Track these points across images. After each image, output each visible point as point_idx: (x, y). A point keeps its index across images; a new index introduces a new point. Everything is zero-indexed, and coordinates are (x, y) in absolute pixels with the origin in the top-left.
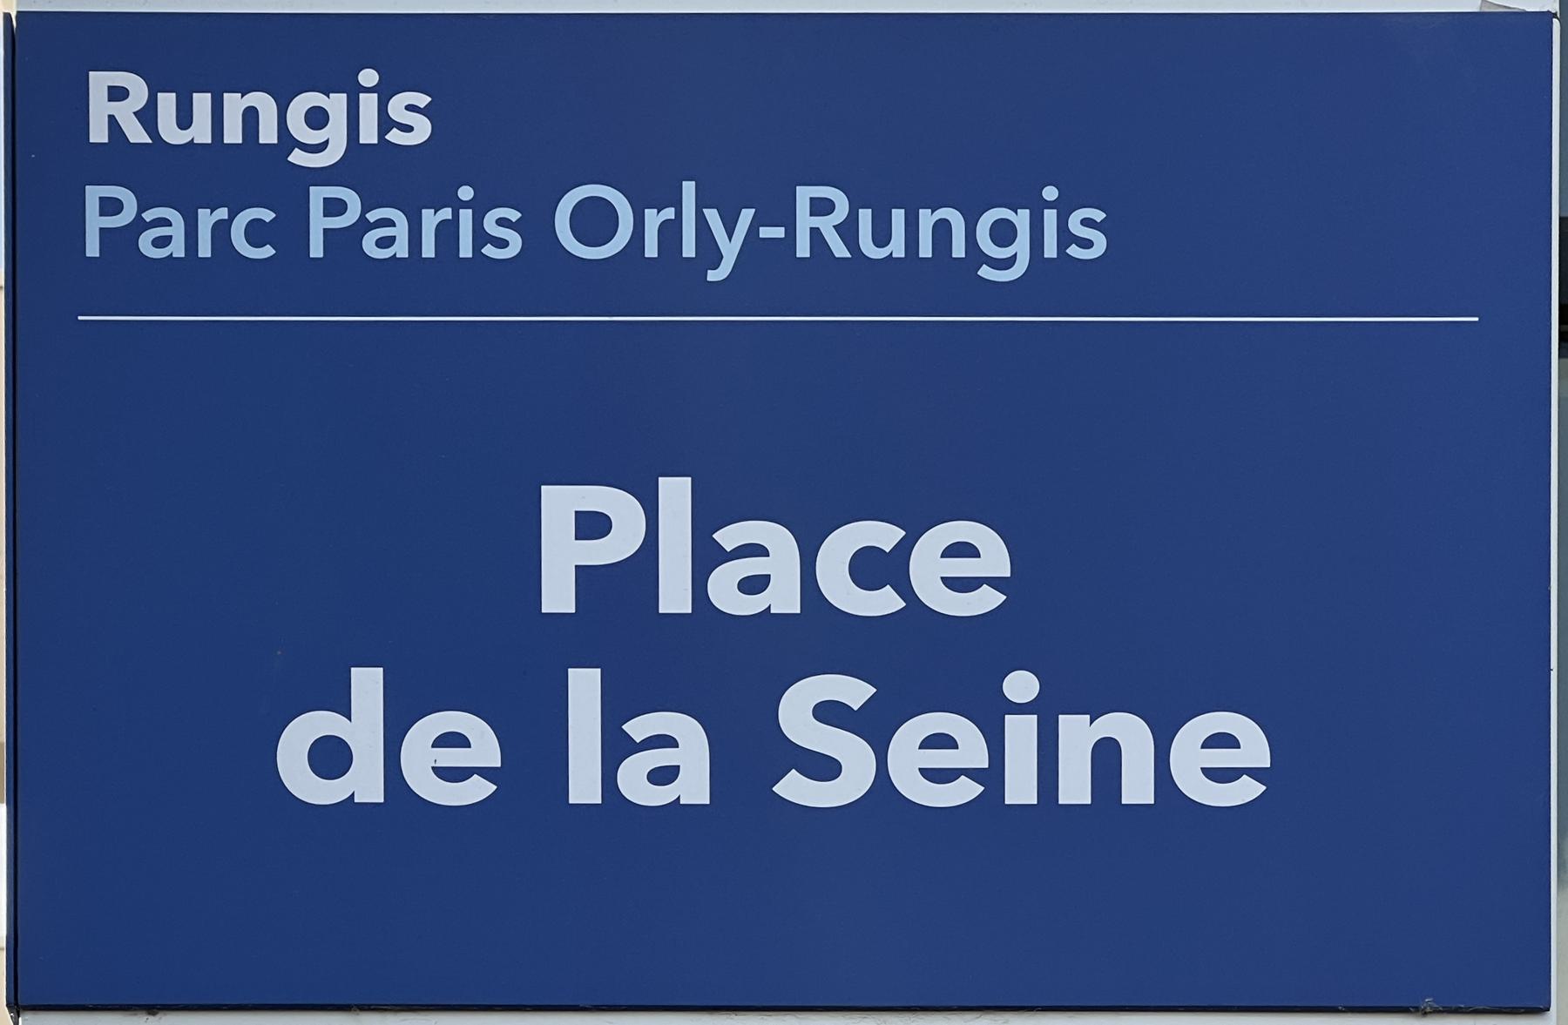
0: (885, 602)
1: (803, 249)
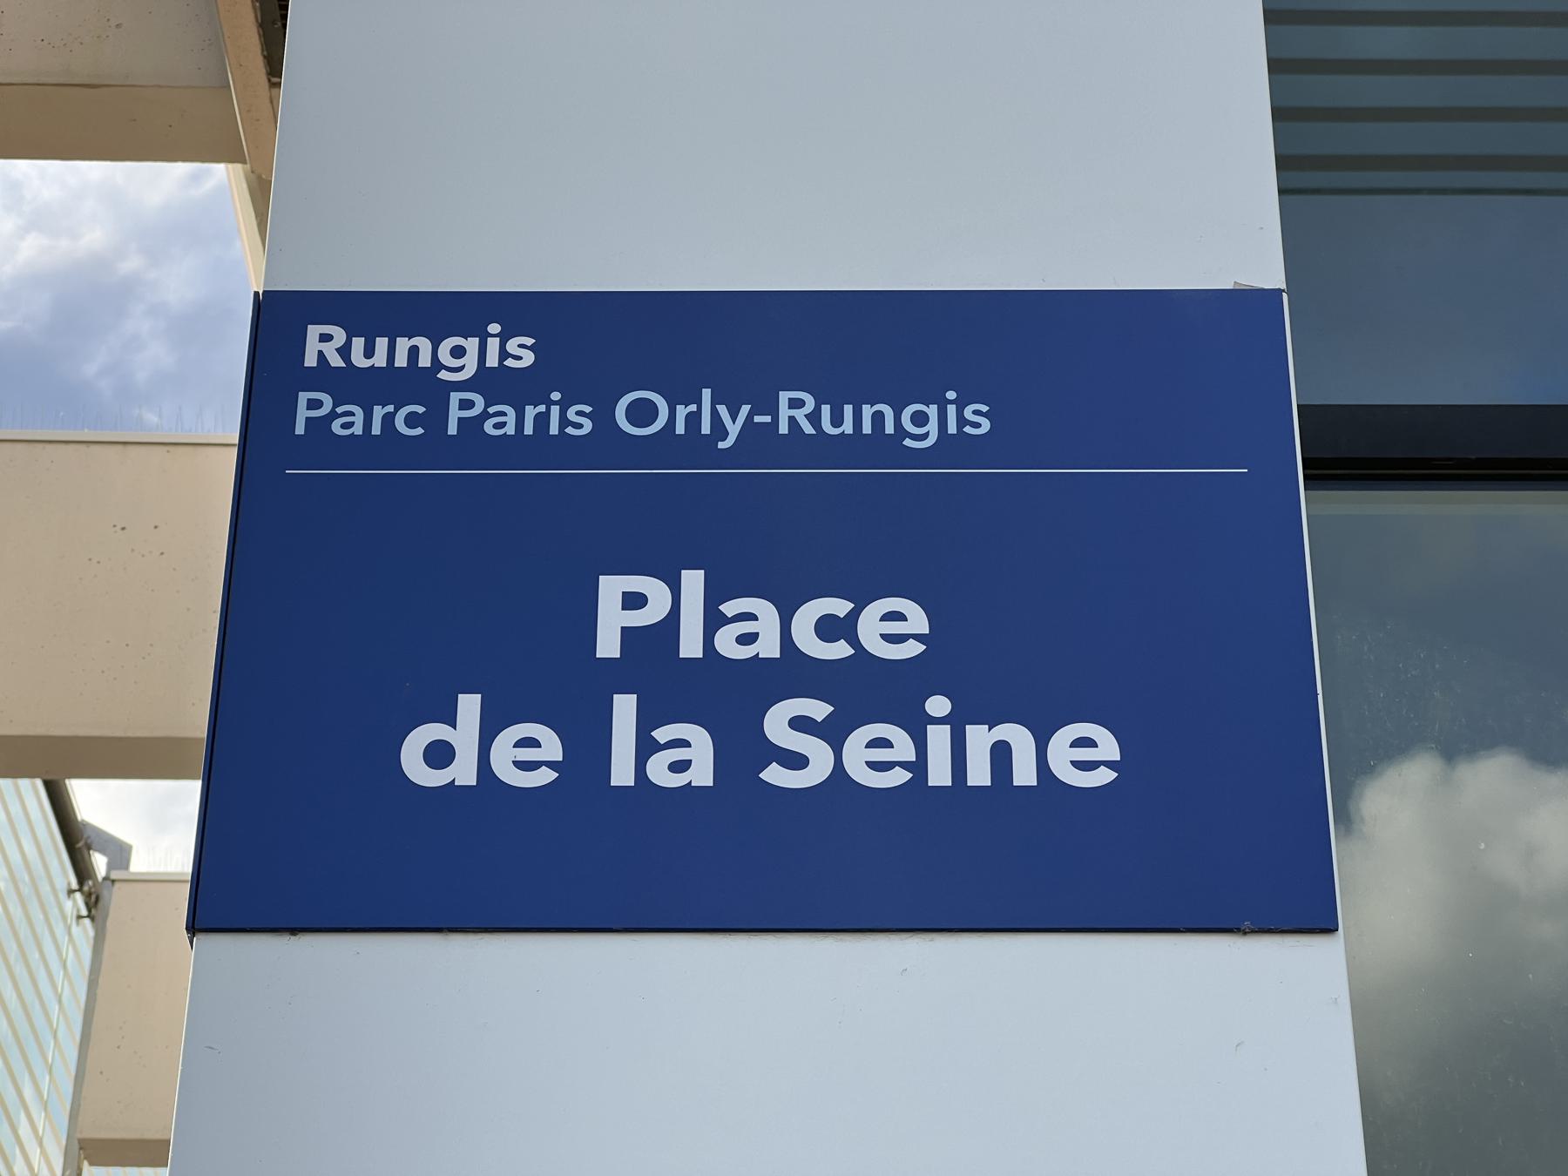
0: (840, 650)
1: (784, 429)
